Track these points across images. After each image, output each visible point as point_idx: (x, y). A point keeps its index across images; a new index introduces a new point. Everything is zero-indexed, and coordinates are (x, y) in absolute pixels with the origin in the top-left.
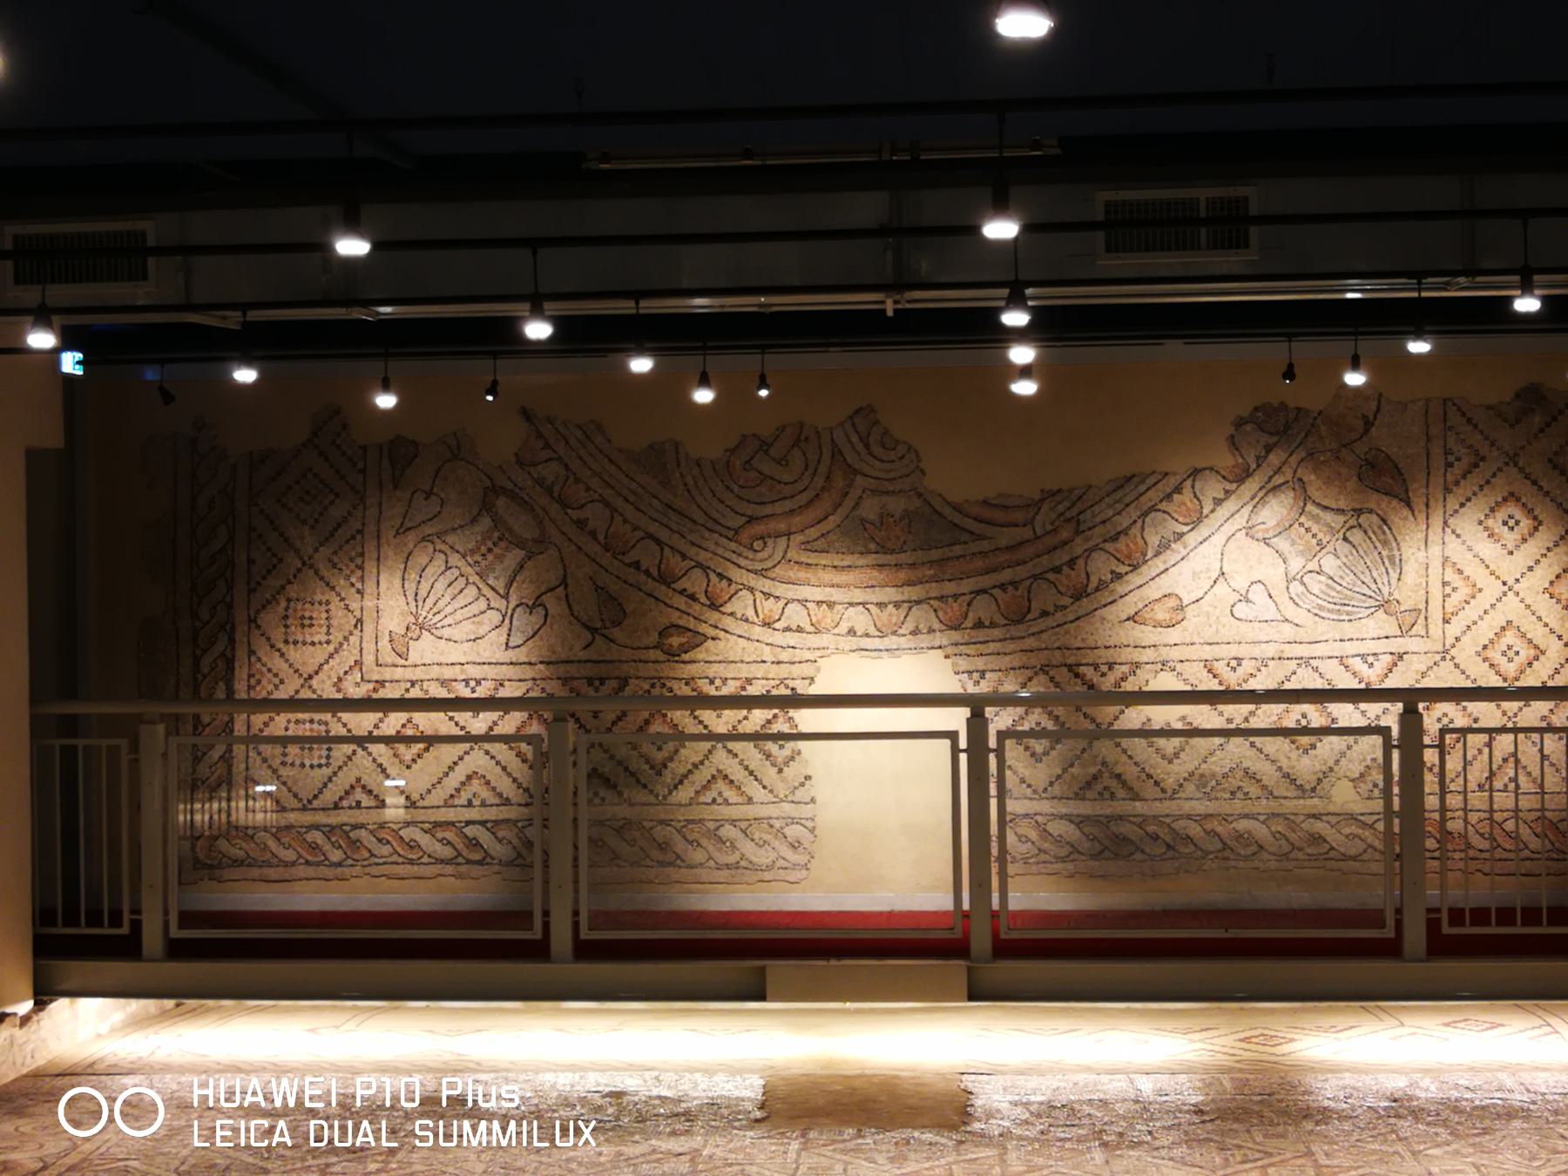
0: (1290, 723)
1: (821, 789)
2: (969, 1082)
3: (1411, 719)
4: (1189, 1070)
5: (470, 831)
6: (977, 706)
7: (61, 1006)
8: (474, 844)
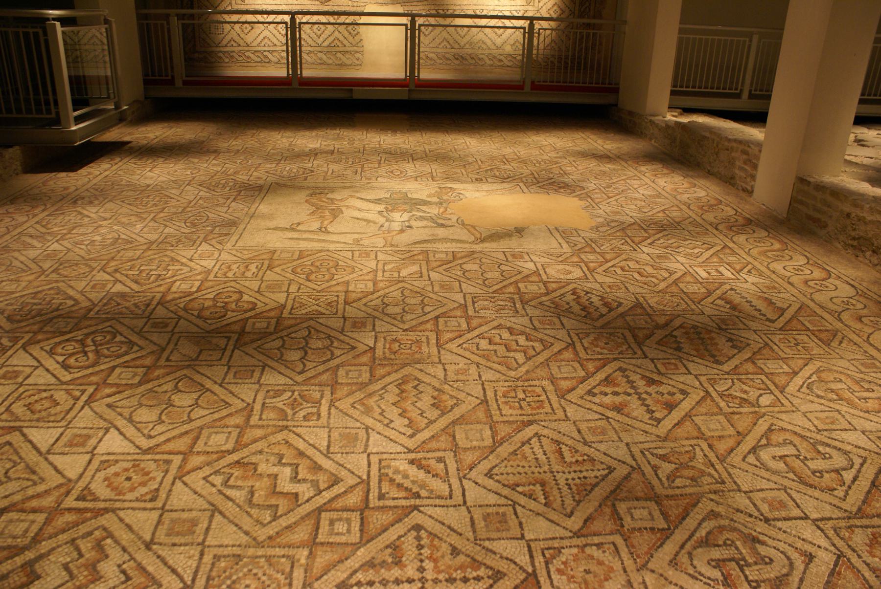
1: (365, 43)
3: (531, 26)
5: (265, 53)
6: (413, 17)
8: (266, 57)
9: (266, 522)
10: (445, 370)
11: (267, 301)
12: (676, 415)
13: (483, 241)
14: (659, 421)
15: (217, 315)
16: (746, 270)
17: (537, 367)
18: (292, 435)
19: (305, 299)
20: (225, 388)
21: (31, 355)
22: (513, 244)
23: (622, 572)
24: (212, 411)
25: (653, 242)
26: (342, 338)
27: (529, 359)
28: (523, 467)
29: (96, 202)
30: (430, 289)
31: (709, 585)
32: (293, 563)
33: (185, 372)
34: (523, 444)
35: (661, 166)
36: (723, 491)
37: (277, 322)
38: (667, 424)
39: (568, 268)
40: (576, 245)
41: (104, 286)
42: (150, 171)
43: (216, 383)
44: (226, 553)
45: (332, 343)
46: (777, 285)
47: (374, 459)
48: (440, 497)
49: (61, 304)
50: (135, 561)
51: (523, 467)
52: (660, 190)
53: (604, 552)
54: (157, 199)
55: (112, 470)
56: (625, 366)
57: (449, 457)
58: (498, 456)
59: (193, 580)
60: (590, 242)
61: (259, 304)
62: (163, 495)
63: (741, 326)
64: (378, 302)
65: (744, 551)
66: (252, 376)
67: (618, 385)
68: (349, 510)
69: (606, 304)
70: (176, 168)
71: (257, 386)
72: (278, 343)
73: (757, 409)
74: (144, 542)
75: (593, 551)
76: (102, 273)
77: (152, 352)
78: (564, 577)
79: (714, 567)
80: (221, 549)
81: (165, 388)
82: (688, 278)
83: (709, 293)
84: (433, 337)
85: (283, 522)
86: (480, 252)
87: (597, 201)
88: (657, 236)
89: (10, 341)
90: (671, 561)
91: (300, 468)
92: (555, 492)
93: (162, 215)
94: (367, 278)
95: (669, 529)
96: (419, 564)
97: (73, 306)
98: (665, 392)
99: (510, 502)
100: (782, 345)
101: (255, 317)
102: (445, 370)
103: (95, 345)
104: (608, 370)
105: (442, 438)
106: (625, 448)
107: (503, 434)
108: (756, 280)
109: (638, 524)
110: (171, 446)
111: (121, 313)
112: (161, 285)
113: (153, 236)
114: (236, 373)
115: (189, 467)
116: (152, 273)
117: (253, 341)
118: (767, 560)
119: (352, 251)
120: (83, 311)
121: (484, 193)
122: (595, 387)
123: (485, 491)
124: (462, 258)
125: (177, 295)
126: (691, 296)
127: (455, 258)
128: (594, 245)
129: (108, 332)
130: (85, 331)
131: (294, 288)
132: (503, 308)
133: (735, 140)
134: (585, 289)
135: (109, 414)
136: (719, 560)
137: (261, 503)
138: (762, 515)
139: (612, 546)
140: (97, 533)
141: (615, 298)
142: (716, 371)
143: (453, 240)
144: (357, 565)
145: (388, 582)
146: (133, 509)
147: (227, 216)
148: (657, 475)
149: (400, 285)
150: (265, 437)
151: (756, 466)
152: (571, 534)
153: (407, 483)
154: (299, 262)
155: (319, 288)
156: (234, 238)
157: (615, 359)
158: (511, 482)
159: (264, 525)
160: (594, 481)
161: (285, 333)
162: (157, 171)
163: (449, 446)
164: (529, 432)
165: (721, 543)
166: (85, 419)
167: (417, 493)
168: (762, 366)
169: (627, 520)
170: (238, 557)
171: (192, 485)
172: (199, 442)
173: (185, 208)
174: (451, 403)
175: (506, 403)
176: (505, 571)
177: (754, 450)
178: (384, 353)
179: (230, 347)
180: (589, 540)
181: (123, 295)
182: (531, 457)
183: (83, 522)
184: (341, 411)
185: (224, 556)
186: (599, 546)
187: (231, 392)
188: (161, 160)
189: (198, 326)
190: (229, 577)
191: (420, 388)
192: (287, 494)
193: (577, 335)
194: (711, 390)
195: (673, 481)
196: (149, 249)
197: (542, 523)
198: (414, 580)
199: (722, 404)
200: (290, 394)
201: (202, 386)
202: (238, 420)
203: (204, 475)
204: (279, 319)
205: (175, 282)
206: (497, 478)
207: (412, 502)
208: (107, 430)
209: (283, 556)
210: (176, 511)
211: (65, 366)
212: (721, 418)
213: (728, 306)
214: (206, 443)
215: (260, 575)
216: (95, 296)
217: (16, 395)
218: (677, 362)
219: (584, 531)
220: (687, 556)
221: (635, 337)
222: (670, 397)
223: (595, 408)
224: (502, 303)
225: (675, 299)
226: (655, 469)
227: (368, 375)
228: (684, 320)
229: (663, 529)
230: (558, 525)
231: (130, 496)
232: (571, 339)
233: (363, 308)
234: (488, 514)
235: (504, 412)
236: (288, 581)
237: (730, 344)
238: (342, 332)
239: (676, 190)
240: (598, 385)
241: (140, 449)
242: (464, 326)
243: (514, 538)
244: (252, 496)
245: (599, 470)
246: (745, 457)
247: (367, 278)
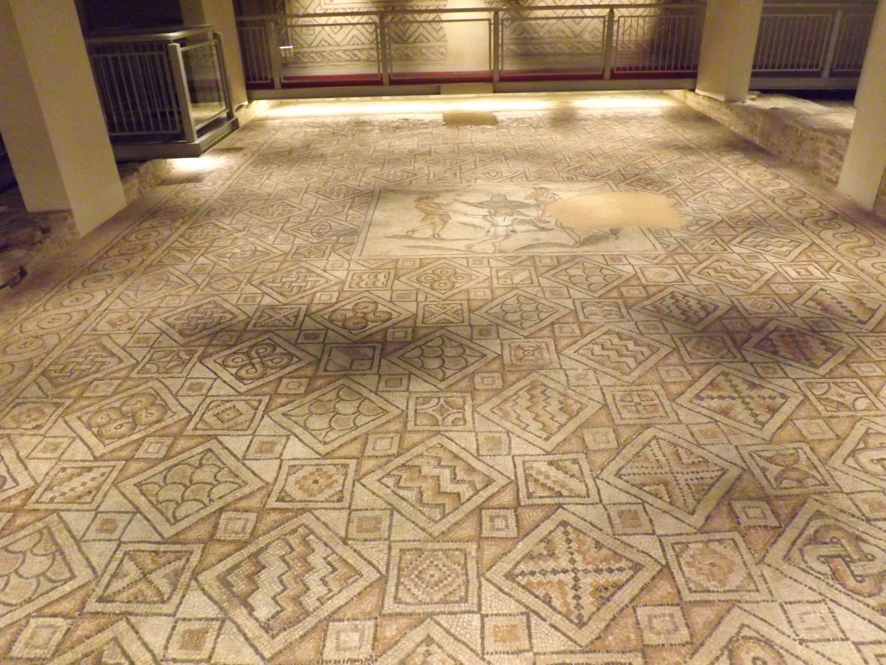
0: (575, 15)
1: (448, 37)
2: (495, 114)
3: (612, 12)
4: (549, 110)
5: (355, 52)
7: (255, 103)
8: (355, 55)
9: (437, 519)
10: (567, 375)
11: (401, 311)
12: (779, 419)
13: (582, 244)
14: (763, 424)
15: (360, 326)
16: (834, 269)
17: (647, 372)
18: (445, 440)
19: (433, 308)
20: (382, 397)
21: (207, 367)
22: (610, 247)
23: (743, 565)
24: (373, 418)
25: (742, 241)
26: (472, 345)
27: (639, 363)
28: (647, 468)
29: (227, 213)
30: (541, 295)
31: (819, 578)
32: (465, 555)
33: (342, 381)
34: (644, 446)
35: (741, 156)
36: (827, 492)
37: (413, 331)
38: (772, 427)
39: (665, 271)
40: (669, 246)
41: (254, 299)
42: (268, 178)
43: (371, 391)
44: (409, 547)
45: (464, 351)
46: (867, 285)
47: (519, 461)
48: (579, 496)
49: (221, 318)
50: (337, 554)
51: (647, 468)
52: (744, 183)
53: (725, 547)
54: (281, 208)
55: (300, 474)
56: (727, 370)
57: (581, 457)
58: (624, 458)
59: (387, 571)
60: (682, 243)
61: (395, 315)
62: (347, 496)
63: (834, 329)
64: (497, 309)
65: (848, 548)
66: (401, 384)
67: (723, 389)
68: (504, 508)
69: (703, 308)
70: (291, 174)
71: (407, 394)
72: (417, 352)
73: (853, 413)
74: (340, 538)
75: (715, 546)
76: (249, 286)
77: (310, 363)
78: (693, 569)
79: (823, 563)
80: (405, 544)
81: (328, 397)
82: (779, 279)
83: (801, 295)
84: (551, 343)
85: (451, 519)
86: (582, 256)
87: (684, 197)
88: (745, 234)
89: (187, 354)
90: (785, 557)
91: (457, 470)
92: (677, 491)
93: (289, 225)
94: (484, 285)
95: (780, 527)
96: (570, 556)
97: (231, 319)
98: (766, 395)
99: (639, 501)
100: (874, 348)
101: (393, 326)
102: (567, 375)
103: (259, 357)
104: (712, 374)
105: (573, 441)
106: (735, 451)
107: (626, 437)
108: (845, 279)
109: (753, 522)
110: (344, 452)
111: (274, 326)
112: (303, 297)
113: (286, 247)
114: (386, 382)
115: (364, 470)
116: (294, 284)
117: (396, 350)
118: (870, 557)
119: (467, 258)
120: (241, 325)
121: (577, 193)
122: (701, 391)
123: (617, 490)
124: (567, 262)
125: (320, 307)
126: (785, 298)
127: (559, 263)
128: (686, 246)
129: (268, 344)
130: (248, 344)
131: (421, 297)
132: (609, 313)
133: (821, 130)
134: (683, 292)
135: (285, 421)
136: (827, 556)
137: (430, 502)
138: (863, 515)
139: (731, 542)
140: (301, 530)
141: (710, 301)
142: (812, 375)
143: (555, 245)
144: (519, 558)
145: (546, 572)
146: (325, 509)
147: (347, 224)
148: (765, 476)
149: (515, 292)
150: (422, 441)
151: (856, 469)
152: (695, 531)
153: (550, 483)
154: (421, 270)
155: (444, 297)
156: (359, 248)
157: (717, 363)
158: (638, 482)
159: (436, 522)
160: (711, 481)
161: (421, 342)
162: (274, 179)
163: (581, 448)
164: (648, 434)
165: (828, 540)
166: (267, 427)
167: (559, 492)
168: (857, 370)
169: (743, 518)
170: (420, 551)
171: (369, 487)
172: (368, 447)
173: (308, 217)
174: (576, 407)
175: (625, 407)
176: (642, 563)
177: (853, 453)
178: (511, 360)
179: (377, 357)
180: (711, 536)
181: (272, 308)
182: (652, 459)
183: (287, 521)
184: (483, 416)
185: (408, 550)
186: (720, 541)
187: (386, 400)
188: (274, 166)
189: (344, 337)
190: (416, 568)
191: (548, 393)
192: (450, 493)
193: (680, 339)
194: (809, 394)
195: (781, 483)
196: (285, 261)
197: (669, 520)
198: (567, 571)
199: (821, 408)
200: (436, 400)
201: (360, 394)
202: (396, 426)
203: (378, 478)
204: (415, 328)
205: (316, 293)
206: (625, 478)
207: (557, 500)
208: (288, 438)
209: (457, 550)
210: (361, 510)
211: (240, 379)
212: (821, 422)
213: (820, 307)
214: (374, 448)
215: (441, 566)
216: (249, 309)
217: (204, 406)
218: (775, 366)
219: (706, 528)
220: (798, 552)
221: (734, 341)
222: (771, 401)
223: (704, 411)
224: (608, 308)
225: (768, 301)
226: (764, 470)
227: (501, 381)
228: (777, 322)
229: (775, 528)
230: (683, 522)
231: (320, 497)
232: (675, 344)
233: (486, 316)
234: (622, 512)
235: (623, 416)
236: (464, 571)
237: (823, 347)
238: (471, 340)
239: (759, 182)
240: (705, 389)
241: (319, 454)
242: (578, 332)
243: (646, 534)
244: (422, 496)
245: (713, 471)
246: (845, 460)
247: (484, 285)
